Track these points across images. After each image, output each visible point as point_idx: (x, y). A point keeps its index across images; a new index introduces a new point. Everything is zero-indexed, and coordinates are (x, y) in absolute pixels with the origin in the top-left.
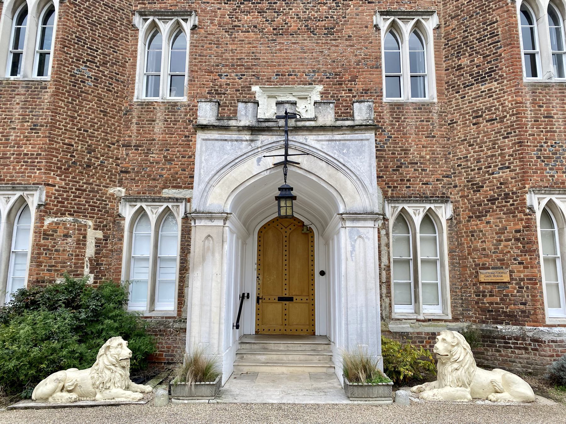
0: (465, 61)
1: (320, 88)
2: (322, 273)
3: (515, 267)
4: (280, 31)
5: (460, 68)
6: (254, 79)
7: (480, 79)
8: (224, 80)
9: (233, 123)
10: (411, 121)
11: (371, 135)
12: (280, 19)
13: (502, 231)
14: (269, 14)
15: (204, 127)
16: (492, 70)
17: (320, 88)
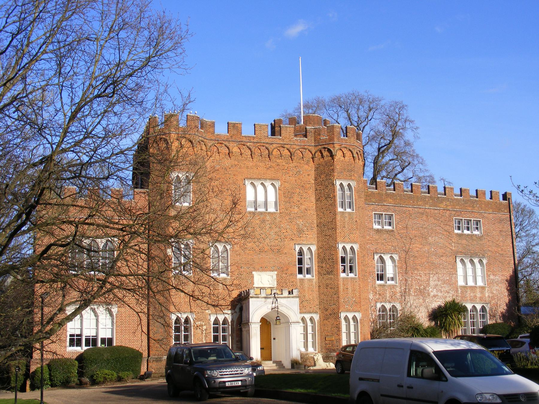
0: (324, 265)
1: (276, 273)
2: (274, 339)
3: (336, 335)
4: (261, 251)
5: (322, 267)
6: (253, 269)
7: (328, 273)
8: (242, 270)
9: (260, 296)
10: (306, 285)
11: (298, 299)
12: (261, 245)
13: (333, 325)
14: (257, 243)
15: (252, 297)
16: (332, 271)
17: (276, 273)
